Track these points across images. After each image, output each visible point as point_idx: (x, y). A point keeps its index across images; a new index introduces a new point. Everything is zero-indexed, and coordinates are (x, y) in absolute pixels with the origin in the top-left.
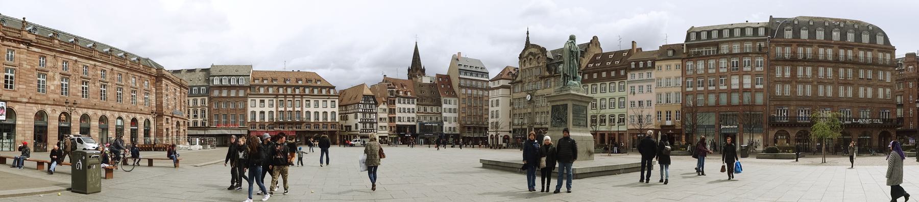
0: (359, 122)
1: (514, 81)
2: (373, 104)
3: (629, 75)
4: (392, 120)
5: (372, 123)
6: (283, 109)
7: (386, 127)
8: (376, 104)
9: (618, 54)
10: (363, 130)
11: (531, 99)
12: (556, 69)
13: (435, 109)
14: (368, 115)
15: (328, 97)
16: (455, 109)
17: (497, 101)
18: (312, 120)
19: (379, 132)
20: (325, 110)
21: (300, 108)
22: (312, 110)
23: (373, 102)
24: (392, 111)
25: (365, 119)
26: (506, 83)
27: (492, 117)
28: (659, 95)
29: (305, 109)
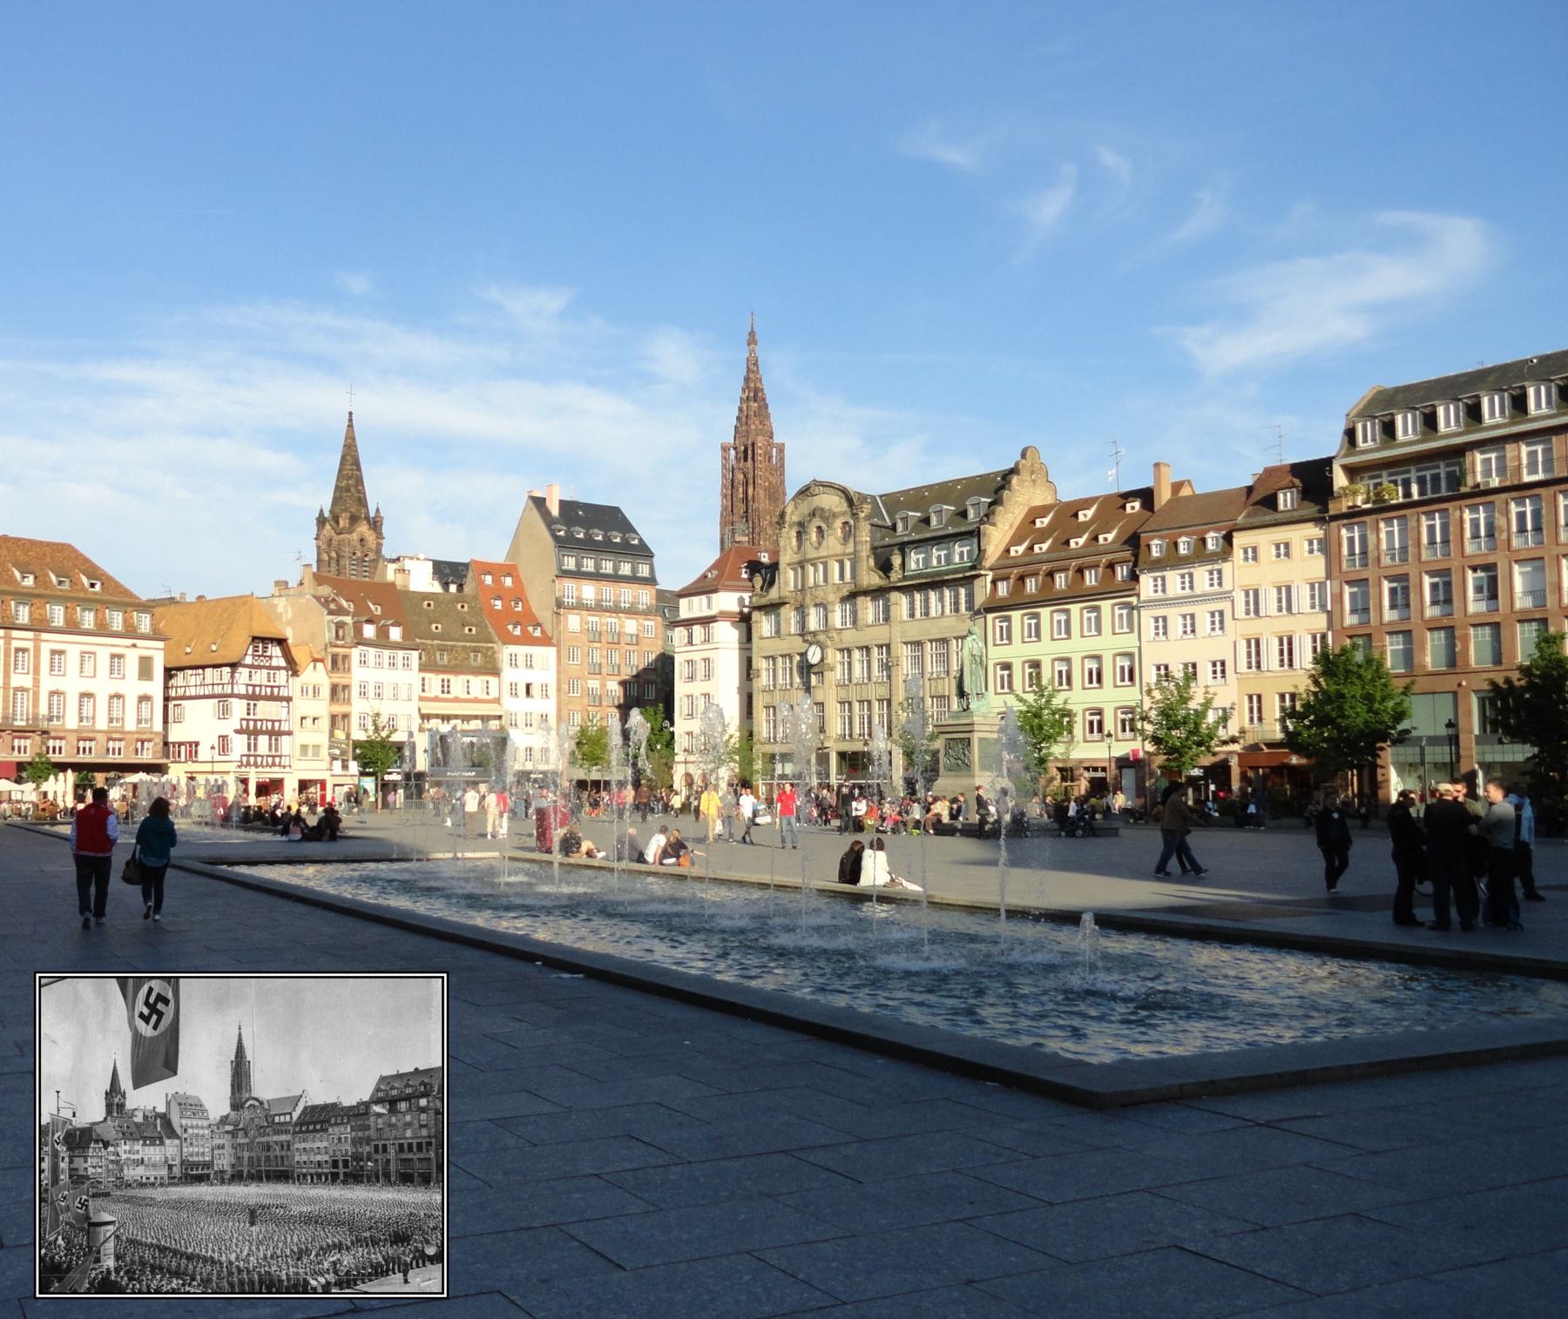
0: (237, 732)
2: (278, 668)
5: (275, 734)
7: (317, 747)
10: (248, 756)
11: (822, 660)
12: (903, 565)
15: (129, 642)
16: (544, 688)
18: (71, 722)
19: (296, 764)
21: (31, 676)
22: (72, 685)
23: (282, 663)
25: (255, 721)
29: (48, 683)
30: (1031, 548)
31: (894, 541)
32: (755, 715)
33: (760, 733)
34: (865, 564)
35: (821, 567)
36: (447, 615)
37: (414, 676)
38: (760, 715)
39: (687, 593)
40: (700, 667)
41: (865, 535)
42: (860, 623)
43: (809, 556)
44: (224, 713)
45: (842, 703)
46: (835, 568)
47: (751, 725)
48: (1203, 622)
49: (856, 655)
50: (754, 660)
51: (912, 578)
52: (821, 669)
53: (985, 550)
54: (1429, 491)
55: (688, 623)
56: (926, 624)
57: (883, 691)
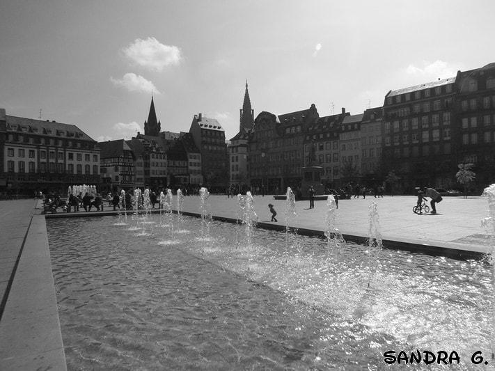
3: (340, 135)
4: (147, 173)
5: (130, 176)
6: (45, 160)
8: (134, 159)
9: (332, 118)
14: (127, 169)
16: (199, 163)
17: (237, 157)
18: (75, 172)
20: (88, 163)
22: (75, 162)
24: (147, 165)
26: (245, 142)
27: (233, 170)
29: (68, 162)
37: (165, 161)
44: (116, 170)
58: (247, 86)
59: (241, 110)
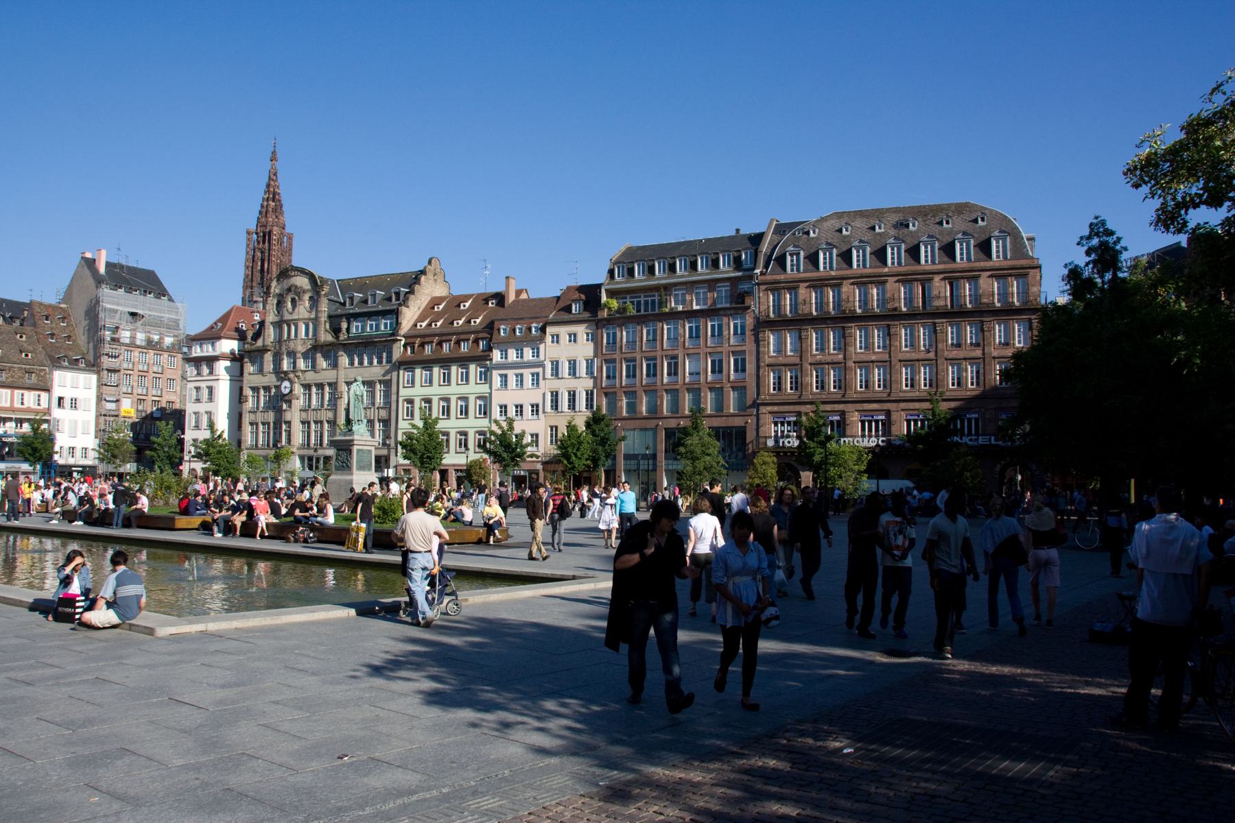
1: (253, 347)
11: (291, 391)
12: (348, 330)
13: (30, 398)
27: (197, 427)
28: (555, 396)
30: (430, 325)
31: (344, 312)
32: (243, 429)
33: (246, 441)
34: (323, 326)
35: (293, 328)
36: (7, 343)
38: (247, 429)
39: (201, 339)
40: (206, 392)
41: (324, 307)
42: (318, 367)
43: (285, 318)
45: (303, 423)
46: (302, 327)
47: (240, 435)
48: (528, 379)
49: (314, 389)
50: (244, 389)
51: (353, 338)
52: (288, 399)
53: (401, 323)
54: (642, 311)
55: (197, 362)
56: (361, 370)
57: (330, 415)
58: (273, 158)
59: (248, 233)
